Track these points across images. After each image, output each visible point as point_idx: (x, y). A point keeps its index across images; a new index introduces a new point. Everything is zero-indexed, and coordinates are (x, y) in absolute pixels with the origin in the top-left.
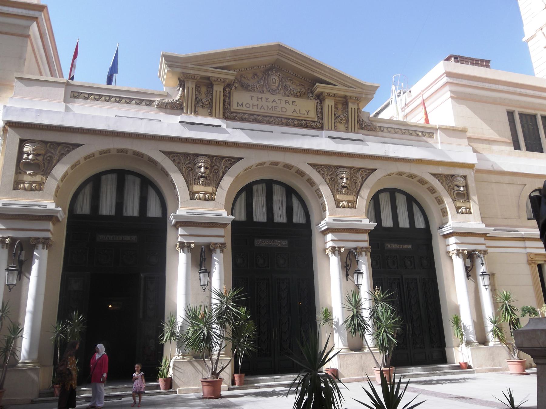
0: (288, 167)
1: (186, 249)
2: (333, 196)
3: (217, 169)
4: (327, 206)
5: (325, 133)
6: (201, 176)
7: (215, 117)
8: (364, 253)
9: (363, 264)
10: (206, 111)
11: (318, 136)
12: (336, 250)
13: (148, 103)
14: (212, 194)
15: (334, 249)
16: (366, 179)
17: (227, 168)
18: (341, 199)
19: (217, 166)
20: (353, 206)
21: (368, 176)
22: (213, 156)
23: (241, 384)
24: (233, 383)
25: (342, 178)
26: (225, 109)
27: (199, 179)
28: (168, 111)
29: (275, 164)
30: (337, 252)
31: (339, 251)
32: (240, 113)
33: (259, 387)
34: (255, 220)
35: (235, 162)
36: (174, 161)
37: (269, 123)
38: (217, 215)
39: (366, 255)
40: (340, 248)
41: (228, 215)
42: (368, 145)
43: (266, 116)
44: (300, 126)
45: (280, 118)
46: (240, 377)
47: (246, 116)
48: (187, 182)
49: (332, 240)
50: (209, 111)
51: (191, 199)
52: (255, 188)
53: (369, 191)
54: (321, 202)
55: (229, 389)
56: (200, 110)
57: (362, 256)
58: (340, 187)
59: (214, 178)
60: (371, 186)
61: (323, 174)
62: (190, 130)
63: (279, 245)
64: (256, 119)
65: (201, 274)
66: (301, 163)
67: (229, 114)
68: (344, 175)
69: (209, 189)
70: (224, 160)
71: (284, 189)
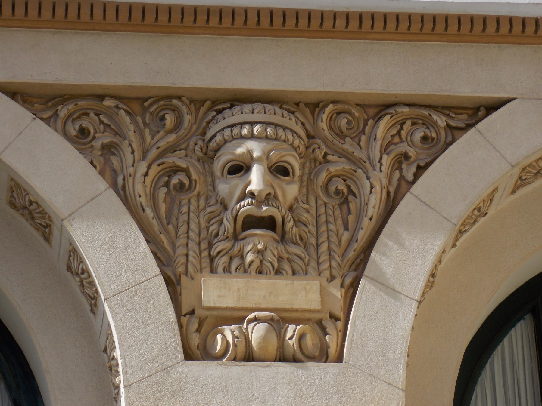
2: (173, 285)
4: (117, 353)
16: (421, 170)
18: (229, 302)
20: (315, 342)
21: (435, 147)
25: (240, 169)
53: (437, 243)
58: (228, 224)
60: (459, 210)
61: (109, 149)
68: (255, 148)
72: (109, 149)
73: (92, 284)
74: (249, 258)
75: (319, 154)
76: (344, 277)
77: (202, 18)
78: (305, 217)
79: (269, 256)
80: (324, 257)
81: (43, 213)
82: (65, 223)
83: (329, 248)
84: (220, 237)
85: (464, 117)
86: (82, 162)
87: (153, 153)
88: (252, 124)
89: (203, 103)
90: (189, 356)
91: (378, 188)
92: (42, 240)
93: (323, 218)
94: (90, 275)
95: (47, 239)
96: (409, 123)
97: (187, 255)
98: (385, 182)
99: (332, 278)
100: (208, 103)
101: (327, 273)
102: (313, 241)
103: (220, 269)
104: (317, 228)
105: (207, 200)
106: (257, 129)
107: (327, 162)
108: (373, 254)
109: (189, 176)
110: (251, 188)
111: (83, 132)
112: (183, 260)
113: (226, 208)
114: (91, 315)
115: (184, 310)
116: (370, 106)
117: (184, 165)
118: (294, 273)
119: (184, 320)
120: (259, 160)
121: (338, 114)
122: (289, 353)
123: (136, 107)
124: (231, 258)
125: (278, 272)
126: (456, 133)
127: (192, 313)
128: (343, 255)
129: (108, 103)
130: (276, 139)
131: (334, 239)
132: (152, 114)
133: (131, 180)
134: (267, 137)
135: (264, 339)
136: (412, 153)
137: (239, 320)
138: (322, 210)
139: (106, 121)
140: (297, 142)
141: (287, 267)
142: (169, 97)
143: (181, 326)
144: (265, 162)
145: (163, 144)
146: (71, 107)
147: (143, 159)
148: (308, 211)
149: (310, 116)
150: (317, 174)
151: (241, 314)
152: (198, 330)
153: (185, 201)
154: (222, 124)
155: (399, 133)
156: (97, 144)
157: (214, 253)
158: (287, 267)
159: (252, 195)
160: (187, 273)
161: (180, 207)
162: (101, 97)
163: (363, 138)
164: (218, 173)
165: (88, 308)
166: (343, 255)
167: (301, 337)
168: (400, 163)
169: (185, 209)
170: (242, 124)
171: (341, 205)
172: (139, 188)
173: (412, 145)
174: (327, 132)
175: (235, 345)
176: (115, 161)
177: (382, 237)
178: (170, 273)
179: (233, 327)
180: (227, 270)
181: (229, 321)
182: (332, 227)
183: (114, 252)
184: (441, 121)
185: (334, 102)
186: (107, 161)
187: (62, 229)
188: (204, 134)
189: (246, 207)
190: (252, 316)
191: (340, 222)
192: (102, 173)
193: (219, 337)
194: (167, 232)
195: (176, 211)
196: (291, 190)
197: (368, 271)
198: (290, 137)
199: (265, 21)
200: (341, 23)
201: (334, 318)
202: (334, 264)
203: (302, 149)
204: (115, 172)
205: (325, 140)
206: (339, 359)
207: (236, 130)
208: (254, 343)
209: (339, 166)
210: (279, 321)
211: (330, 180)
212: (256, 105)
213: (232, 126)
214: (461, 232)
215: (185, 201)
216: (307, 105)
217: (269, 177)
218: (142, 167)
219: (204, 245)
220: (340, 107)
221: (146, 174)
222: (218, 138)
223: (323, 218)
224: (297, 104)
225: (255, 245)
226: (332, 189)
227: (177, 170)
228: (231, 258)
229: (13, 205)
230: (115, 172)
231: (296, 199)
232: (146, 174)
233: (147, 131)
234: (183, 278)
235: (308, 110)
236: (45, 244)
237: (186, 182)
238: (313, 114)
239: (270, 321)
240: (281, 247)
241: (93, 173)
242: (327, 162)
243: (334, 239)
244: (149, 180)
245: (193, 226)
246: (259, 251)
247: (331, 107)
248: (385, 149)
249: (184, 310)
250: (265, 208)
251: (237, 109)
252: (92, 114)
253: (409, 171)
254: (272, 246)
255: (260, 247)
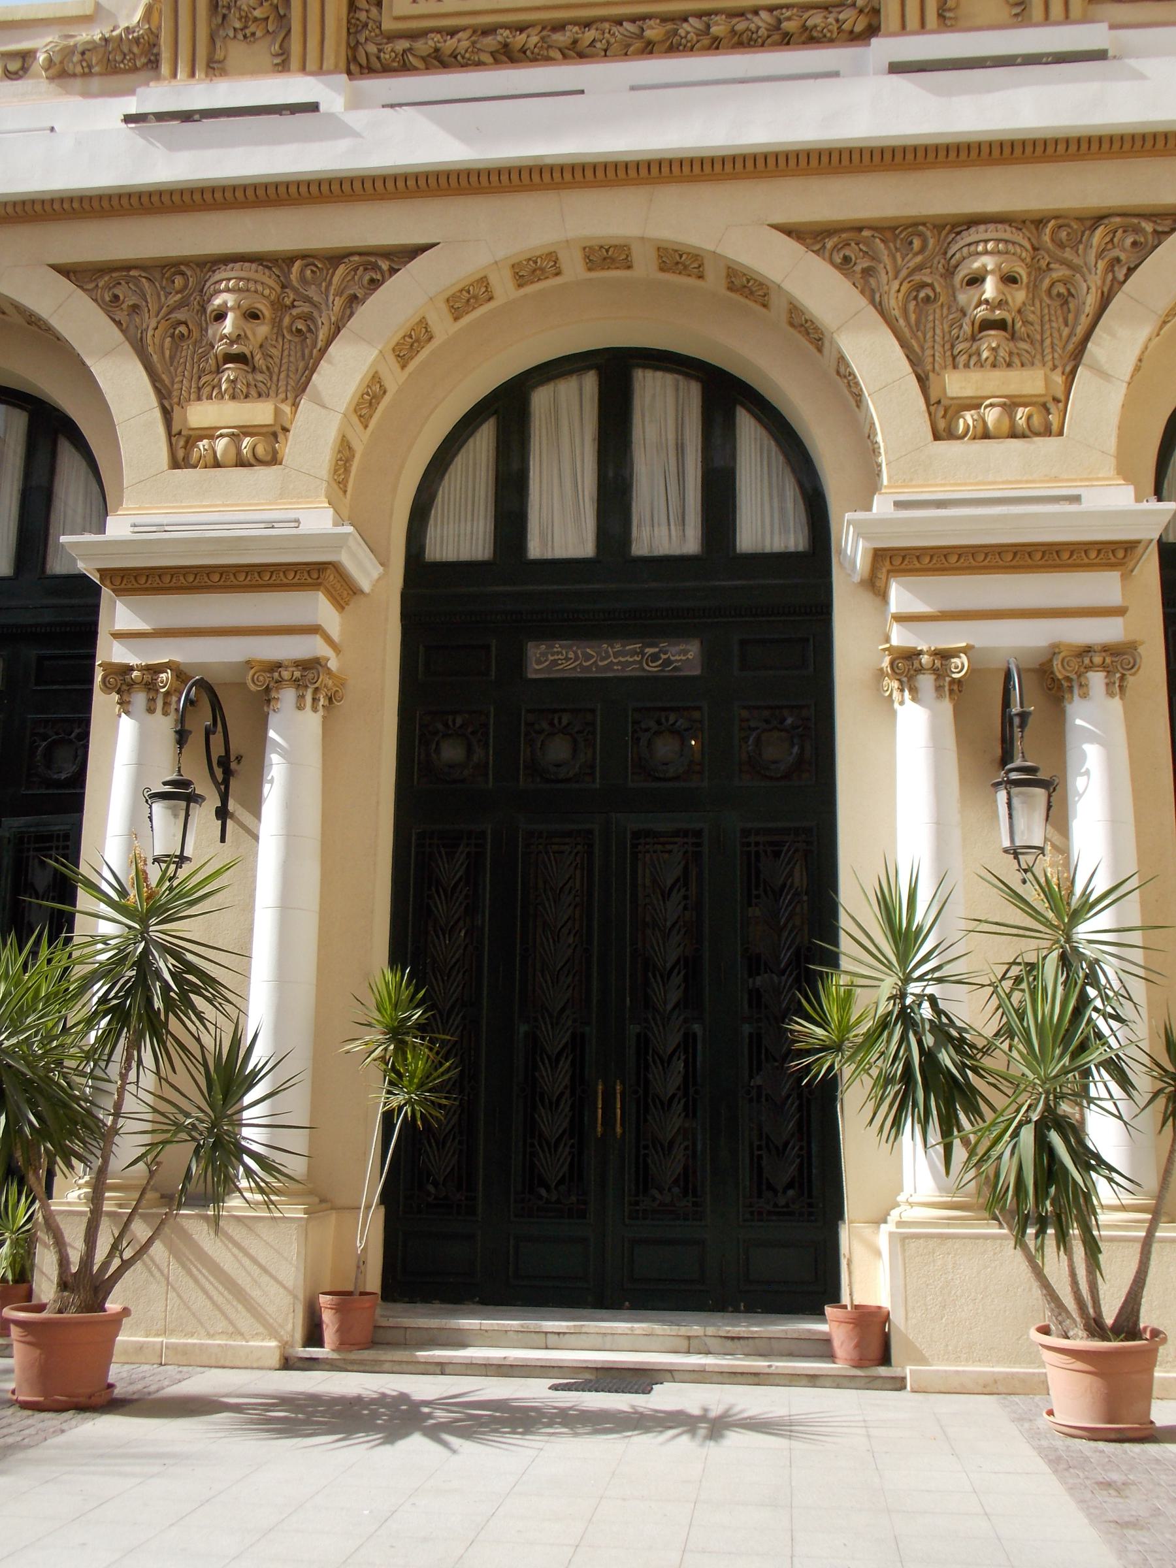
0: (679, 261)
1: (139, 699)
2: (922, 380)
3: (307, 318)
4: (879, 438)
5: (884, 48)
6: (229, 358)
7: (303, 69)
8: (1097, 680)
9: (1092, 738)
10: (264, 50)
11: (836, 74)
12: (921, 670)
13: (14, 66)
14: (275, 435)
15: (906, 666)
16: (1131, 271)
17: (354, 301)
18: (969, 392)
19: (308, 300)
21: (1143, 250)
22: (289, 259)
23: (344, 1343)
24: (314, 1337)
25: (976, 280)
26: (354, 27)
27: (219, 371)
28: (95, 83)
29: (607, 256)
30: (926, 682)
31: (940, 673)
32: (423, 33)
33: (442, 1368)
34: (535, 549)
35: (393, 271)
36: (111, 305)
37: (577, 53)
38: (271, 525)
39: (1118, 687)
40: (944, 655)
41: (335, 525)
42: (1142, 77)
43: (559, 27)
44: (744, 42)
45: (633, 20)
46: (339, 1309)
47: (462, 42)
48: (163, 393)
49: (900, 618)
50: (276, 48)
51: (175, 464)
52: (541, 398)
54: (866, 431)
55: (288, 1364)
56: (236, 51)
57: (1085, 696)
58: (967, 328)
59: (284, 358)
61: (868, 272)
62: (172, 147)
63: (653, 668)
64: (506, 45)
65: (158, 808)
66: (738, 231)
67: (372, 48)
68: (989, 262)
69: (260, 412)
70: (341, 269)
71: (693, 392)
72: (868, 272)
73: (857, 384)
74: (985, 355)
75: (1043, 264)
76: (1064, 367)
77: (942, 154)
78: (1031, 317)
79: (1002, 353)
80: (1048, 350)
81: (816, 329)
82: (835, 335)
83: (1052, 343)
84: (960, 339)
85: (1169, 222)
86: (847, 284)
87: (904, 273)
88: (986, 241)
89: (944, 227)
90: (937, 437)
91: (1093, 290)
92: (815, 351)
93: (1047, 318)
94: (855, 377)
95: (820, 350)
96: (1120, 231)
97: (934, 356)
98: (1099, 283)
99: (1055, 367)
100: (948, 227)
101: (1050, 364)
102: (1038, 337)
103: (961, 366)
104: (1042, 326)
105: (949, 309)
106: (990, 246)
107: (1051, 269)
108: (1089, 345)
109: (934, 290)
110: (986, 296)
111: (846, 259)
112: (930, 359)
113: (965, 315)
114: (856, 409)
115: (933, 400)
116: (1087, 219)
117: (929, 281)
118: (1022, 365)
119: (932, 408)
120: (992, 272)
121: (1060, 227)
122: (1019, 430)
123: (889, 235)
124: (970, 356)
125: (1009, 365)
126: (1162, 237)
127: (939, 402)
128: (1064, 348)
129: (866, 233)
130: (1006, 253)
131: (1056, 335)
132: (902, 240)
133: (886, 296)
134: (999, 252)
135: (998, 421)
136: (1123, 256)
137: (977, 407)
138: (1046, 311)
139: (864, 249)
140: (1024, 254)
141: (1016, 360)
142: (916, 225)
143: (930, 414)
144: (998, 274)
145: (911, 264)
146: (835, 239)
147: (896, 278)
148: (1033, 312)
149: (1034, 231)
150: (1042, 281)
151: (979, 401)
152: (944, 417)
153: (931, 311)
154: (961, 243)
155: (1112, 240)
156: (858, 268)
157: (956, 352)
158: (1016, 360)
159: (987, 302)
160: (934, 370)
161: (926, 317)
162: (860, 229)
163: (1081, 247)
164: (958, 286)
165: (854, 404)
166: (1064, 348)
167: (1029, 418)
168: (1113, 266)
169: (931, 318)
170: (977, 243)
171: (1062, 305)
172: (893, 303)
173: (1123, 250)
174: (1050, 245)
175: (974, 427)
176: (872, 281)
177: (1097, 330)
178: (920, 371)
179: (973, 412)
180: (967, 366)
181: (969, 408)
182: (1054, 325)
183: (874, 357)
184: (1148, 227)
185: (1056, 218)
186: (867, 282)
187: (832, 341)
188: (945, 253)
189: (981, 312)
190: (988, 402)
191: (1061, 320)
192: (862, 292)
193: (961, 421)
194: (917, 338)
195: (923, 320)
196: (1019, 296)
197: (1086, 358)
198: (1019, 251)
199: (996, 152)
200: (1061, 148)
201: (1056, 400)
202: (1056, 355)
203: (1028, 260)
204: (873, 291)
205: (1048, 251)
206: (1061, 433)
207: (972, 248)
208: (990, 424)
209: (1060, 272)
210: (1010, 406)
211: (1052, 285)
212: (989, 225)
213: (969, 245)
214: (1165, 323)
215: (931, 311)
216: (1032, 222)
217: (1001, 286)
218: (895, 285)
219: (947, 346)
220: (1060, 221)
221: (899, 291)
222: (958, 256)
223: (1047, 318)
224: (1024, 222)
225: (989, 344)
226: (1054, 292)
227: (924, 285)
228: (970, 356)
229: (792, 325)
230: (873, 291)
231: (1024, 304)
232: (899, 291)
233: (898, 255)
234: (931, 374)
235: (1032, 227)
236: (818, 354)
237: (932, 295)
238: (1037, 229)
239: (1003, 405)
240: (1011, 344)
241: (855, 292)
242: (1051, 269)
243: (1056, 335)
244: (901, 295)
245: (938, 331)
246: (993, 349)
247: (1052, 222)
248: (1100, 256)
249: (933, 400)
250: (998, 312)
251: (973, 230)
252: (853, 244)
253: (1119, 273)
254: (1004, 344)
255: (994, 345)
